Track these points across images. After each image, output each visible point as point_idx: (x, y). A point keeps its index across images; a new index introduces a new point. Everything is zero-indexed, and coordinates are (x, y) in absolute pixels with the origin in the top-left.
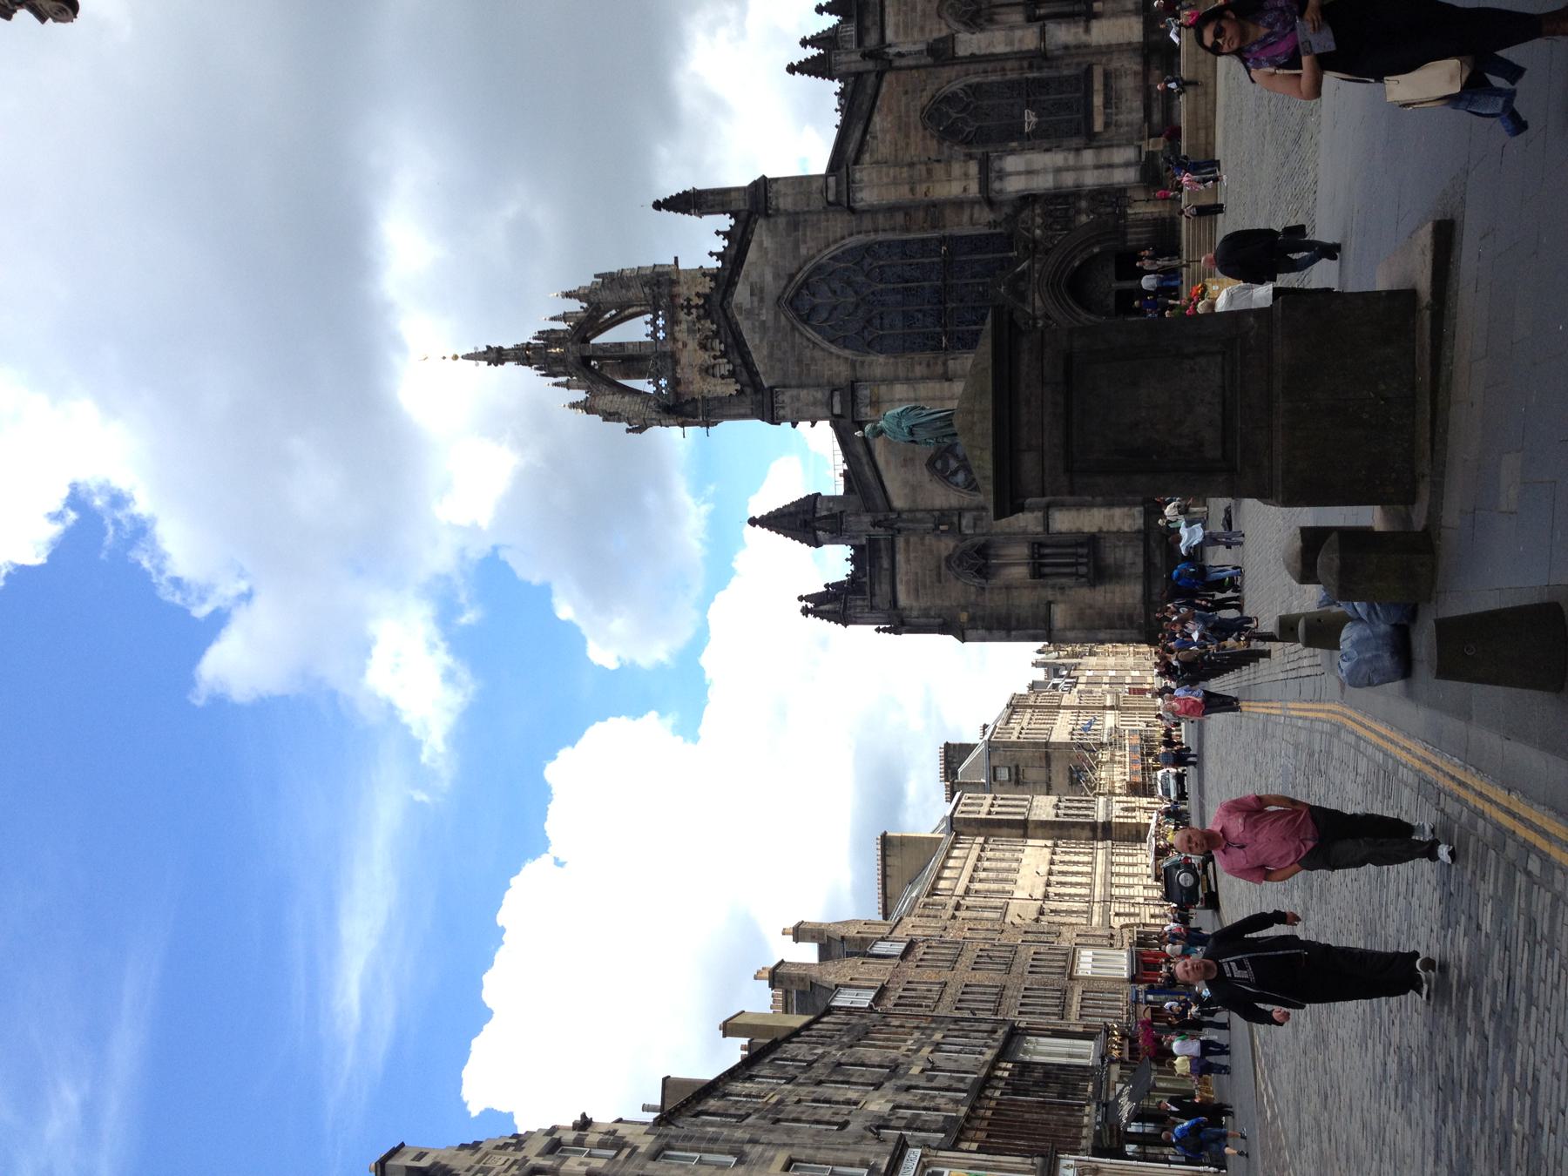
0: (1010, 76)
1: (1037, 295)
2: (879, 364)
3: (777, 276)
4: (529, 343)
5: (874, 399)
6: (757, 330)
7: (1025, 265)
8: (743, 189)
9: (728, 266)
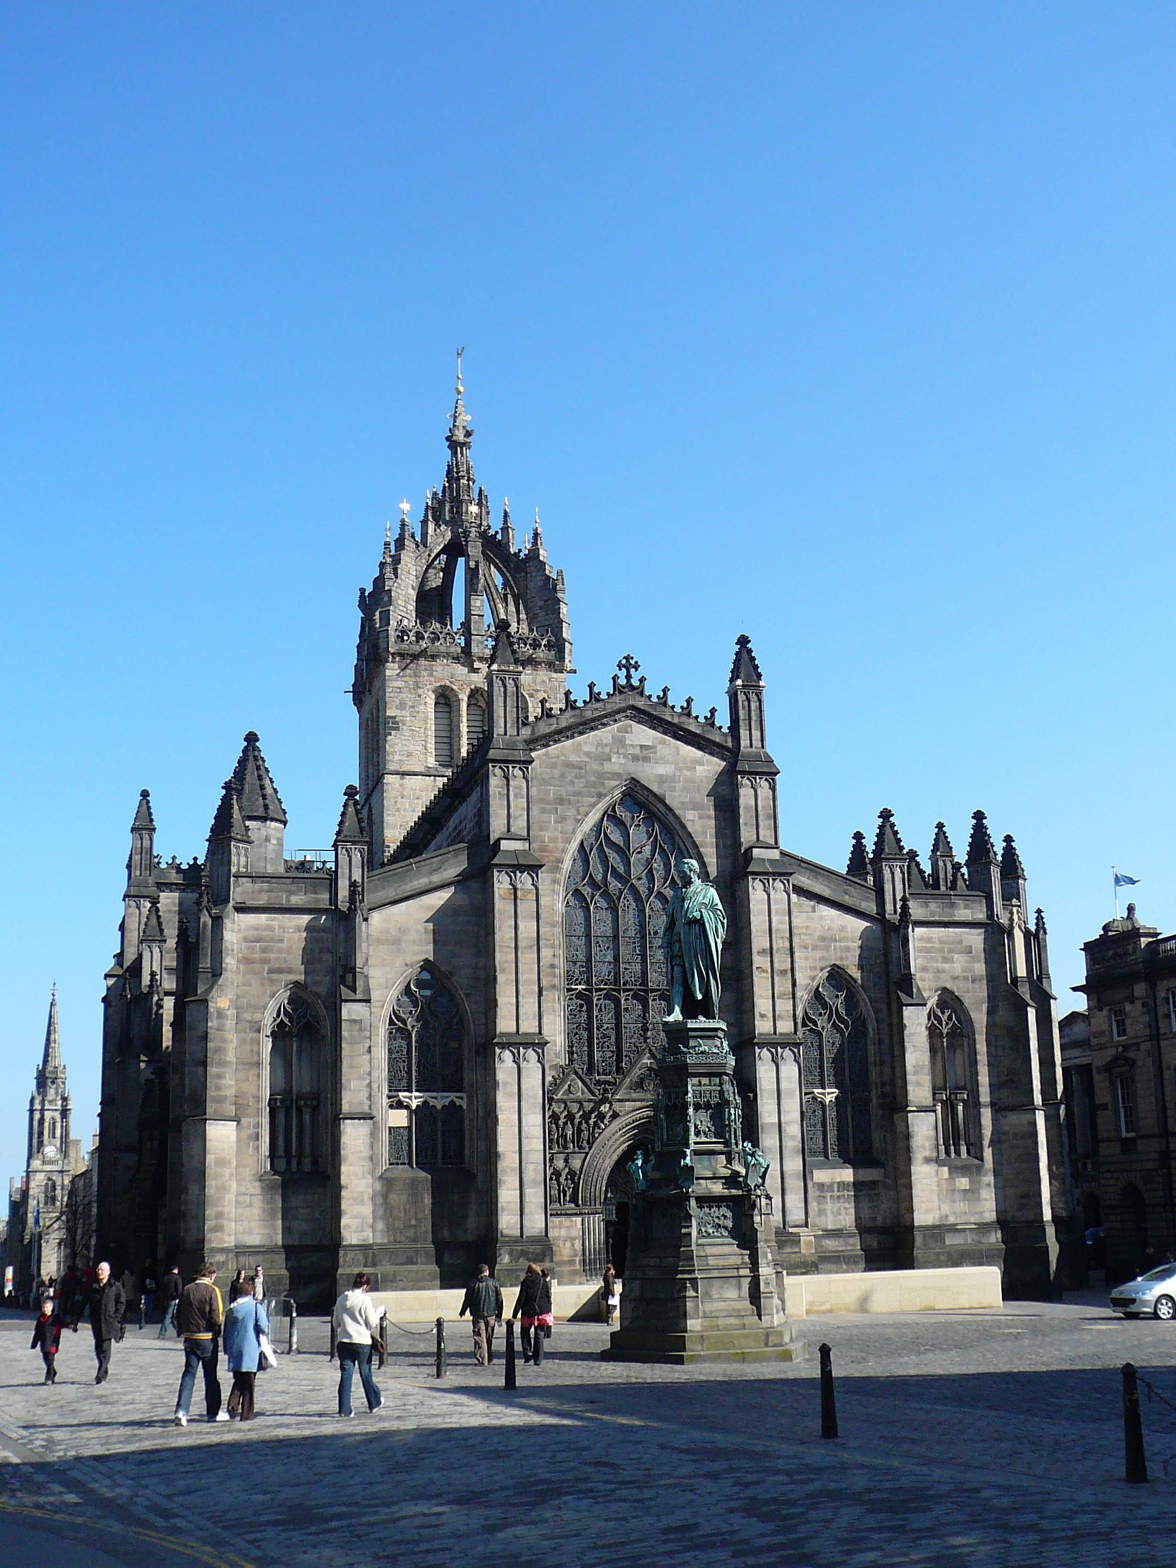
0: (874, 1072)
1: (639, 1104)
2: (556, 902)
3: (662, 779)
4: (473, 483)
5: (519, 893)
6: (600, 749)
8: (763, 747)
9: (676, 720)
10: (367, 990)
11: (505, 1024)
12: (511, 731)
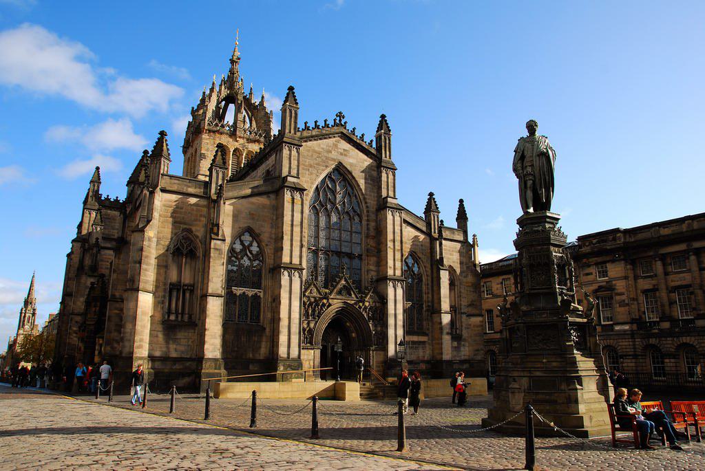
0: (425, 296)
1: (339, 301)
3: (351, 165)
5: (295, 200)
7: (353, 296)
8: (390, 158)
9: (358, 141)
10: (223, 235)
11: (286, 259)
12: (292, 131)
